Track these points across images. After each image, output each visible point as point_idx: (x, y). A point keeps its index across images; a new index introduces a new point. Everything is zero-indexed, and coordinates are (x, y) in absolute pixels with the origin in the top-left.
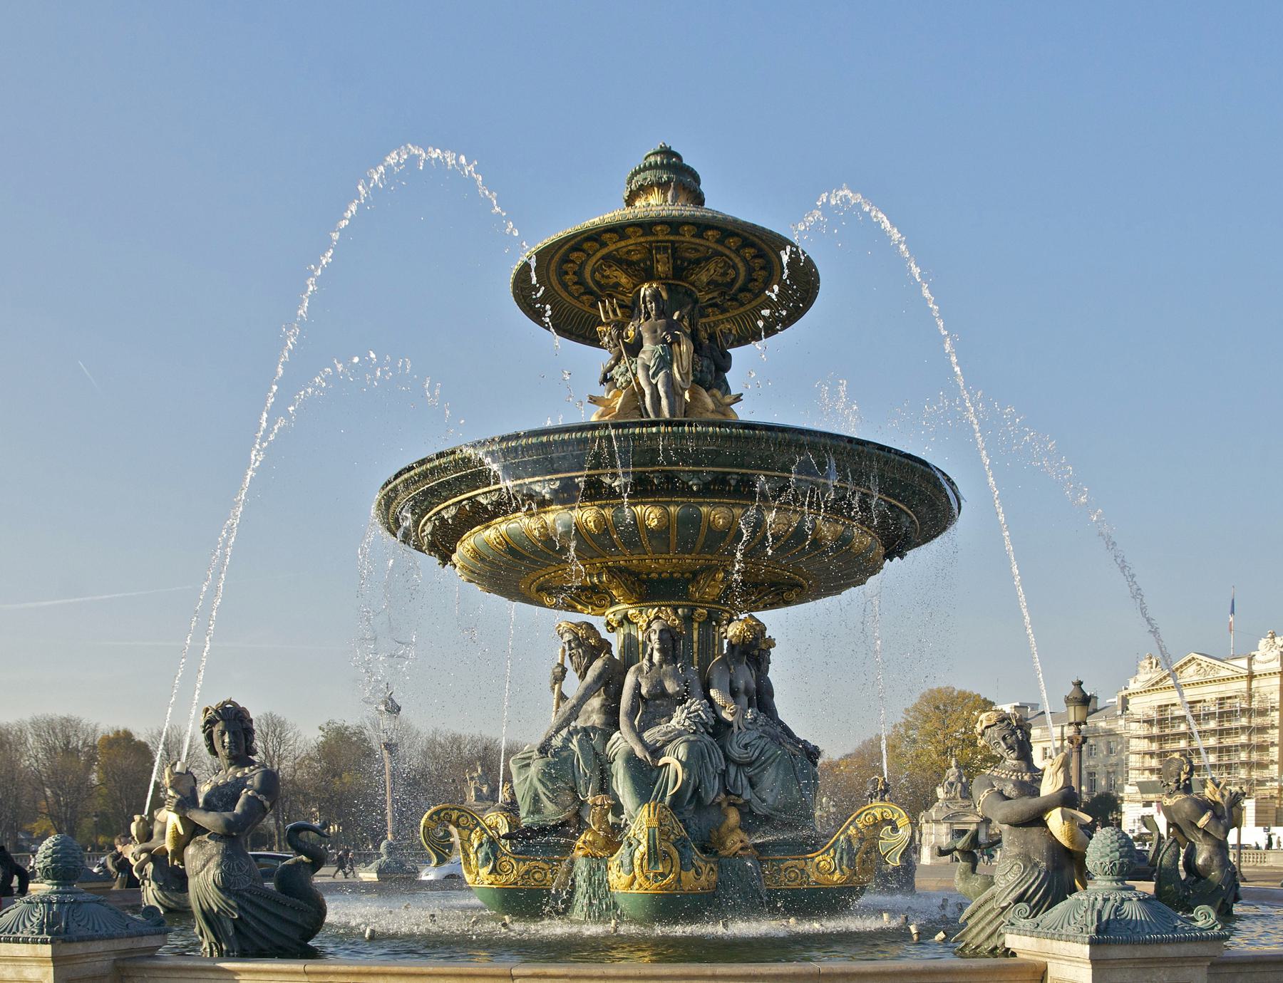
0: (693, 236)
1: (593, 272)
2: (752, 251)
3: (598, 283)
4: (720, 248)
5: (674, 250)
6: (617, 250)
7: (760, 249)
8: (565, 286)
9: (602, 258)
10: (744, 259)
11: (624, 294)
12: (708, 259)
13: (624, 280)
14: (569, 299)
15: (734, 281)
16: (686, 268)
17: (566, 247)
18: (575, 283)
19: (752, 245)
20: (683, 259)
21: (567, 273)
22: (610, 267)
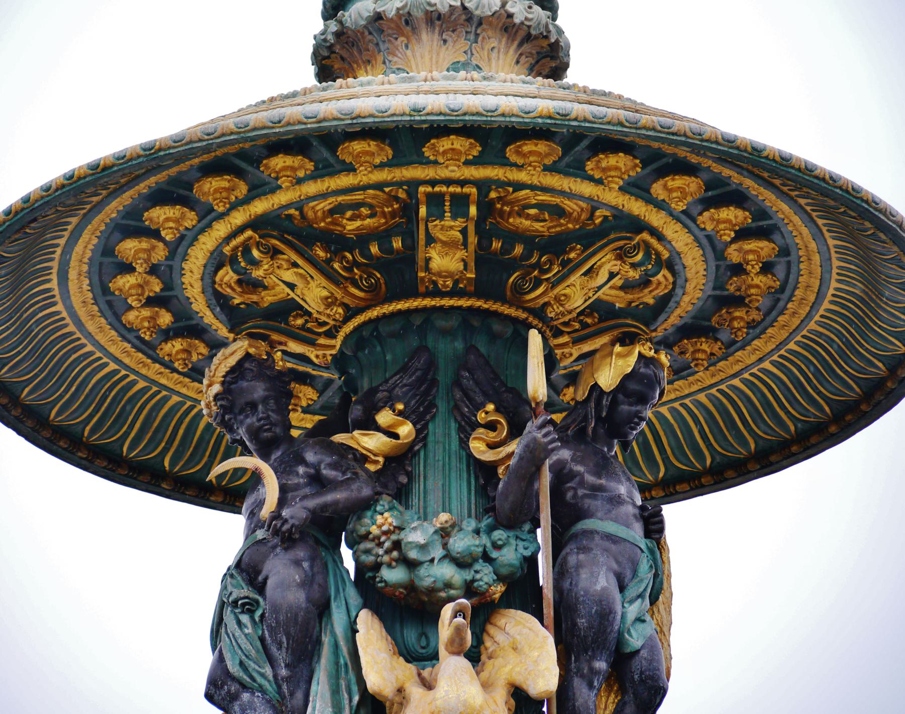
0: (547, 169)
1: (217, 261)
2: (732, 215)
3: (220, 301)
4: (636, 207)
5: (487, 208)
6: (299, 205)
7: (761, 214)
8: (112, 307)
9: (255, 224)
10: (713, 246)
11: (307, 337)
12: (591, 237)
13: (314, 293)
14: (118, 347)
15: (664, 303)
16: (512, 265)
17: (143, 187)
18: (151, 302)
19: (738, 199)
20: (512, 237)
21: (127, 268)
22: (274, 253)
